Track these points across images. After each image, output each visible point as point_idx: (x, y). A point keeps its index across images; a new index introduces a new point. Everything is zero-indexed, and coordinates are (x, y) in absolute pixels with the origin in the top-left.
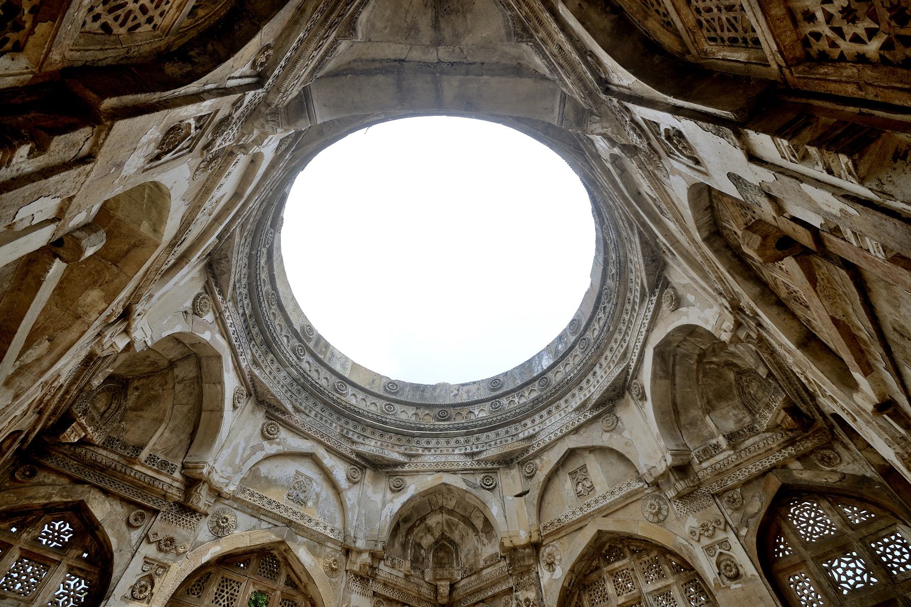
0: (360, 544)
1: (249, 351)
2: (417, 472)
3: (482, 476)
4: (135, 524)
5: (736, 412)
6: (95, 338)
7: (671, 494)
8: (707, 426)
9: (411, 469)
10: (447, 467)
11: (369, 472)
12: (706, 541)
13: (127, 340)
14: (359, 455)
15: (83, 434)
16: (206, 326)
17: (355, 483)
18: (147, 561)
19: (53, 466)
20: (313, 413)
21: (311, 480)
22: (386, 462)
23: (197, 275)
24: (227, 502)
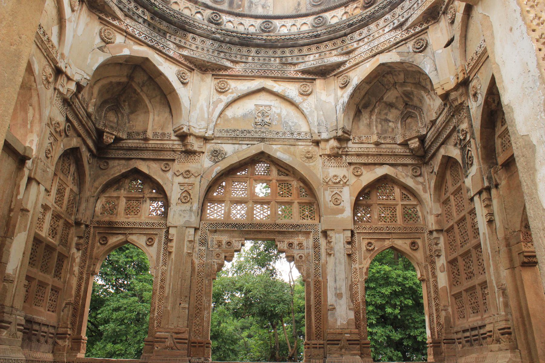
0: (324, 136)
1: (169, 43)
2: (357, 64)
3: (412, 42)
4: (166, 169)
6: (55, 92)
9: (352, 64)
10: (381, 48)
11: (319, 82)
13: (74, 83)
14: (303, 72)
15: (114, 137)
16: (121, 47)
17: (309, 95)
18: (181, 184)
19: (113, 156)
20: (250, 58)
21: (270, 106)
22: (330, 68)
23: (88, 19)
24: (213, 141)
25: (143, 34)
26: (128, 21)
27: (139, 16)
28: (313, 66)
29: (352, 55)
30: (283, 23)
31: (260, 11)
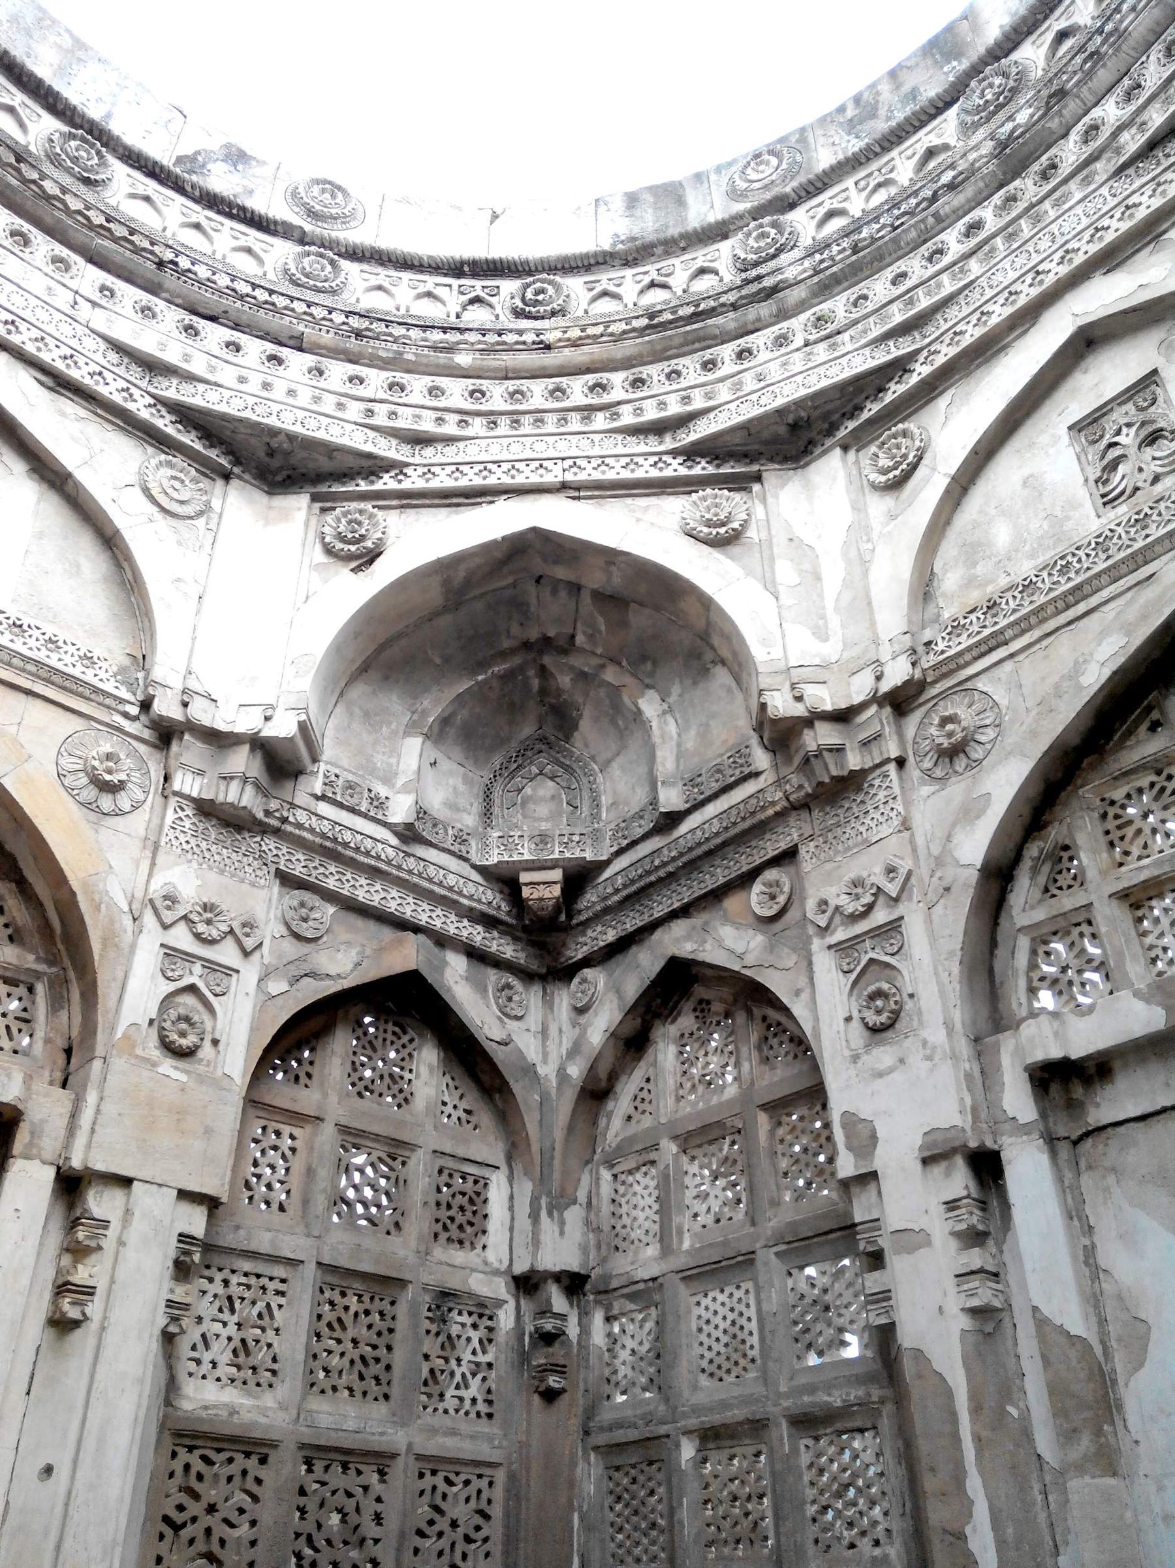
5: (462, 788)
7: (187, 783)
8: (395, 752)
12: (181, 938)
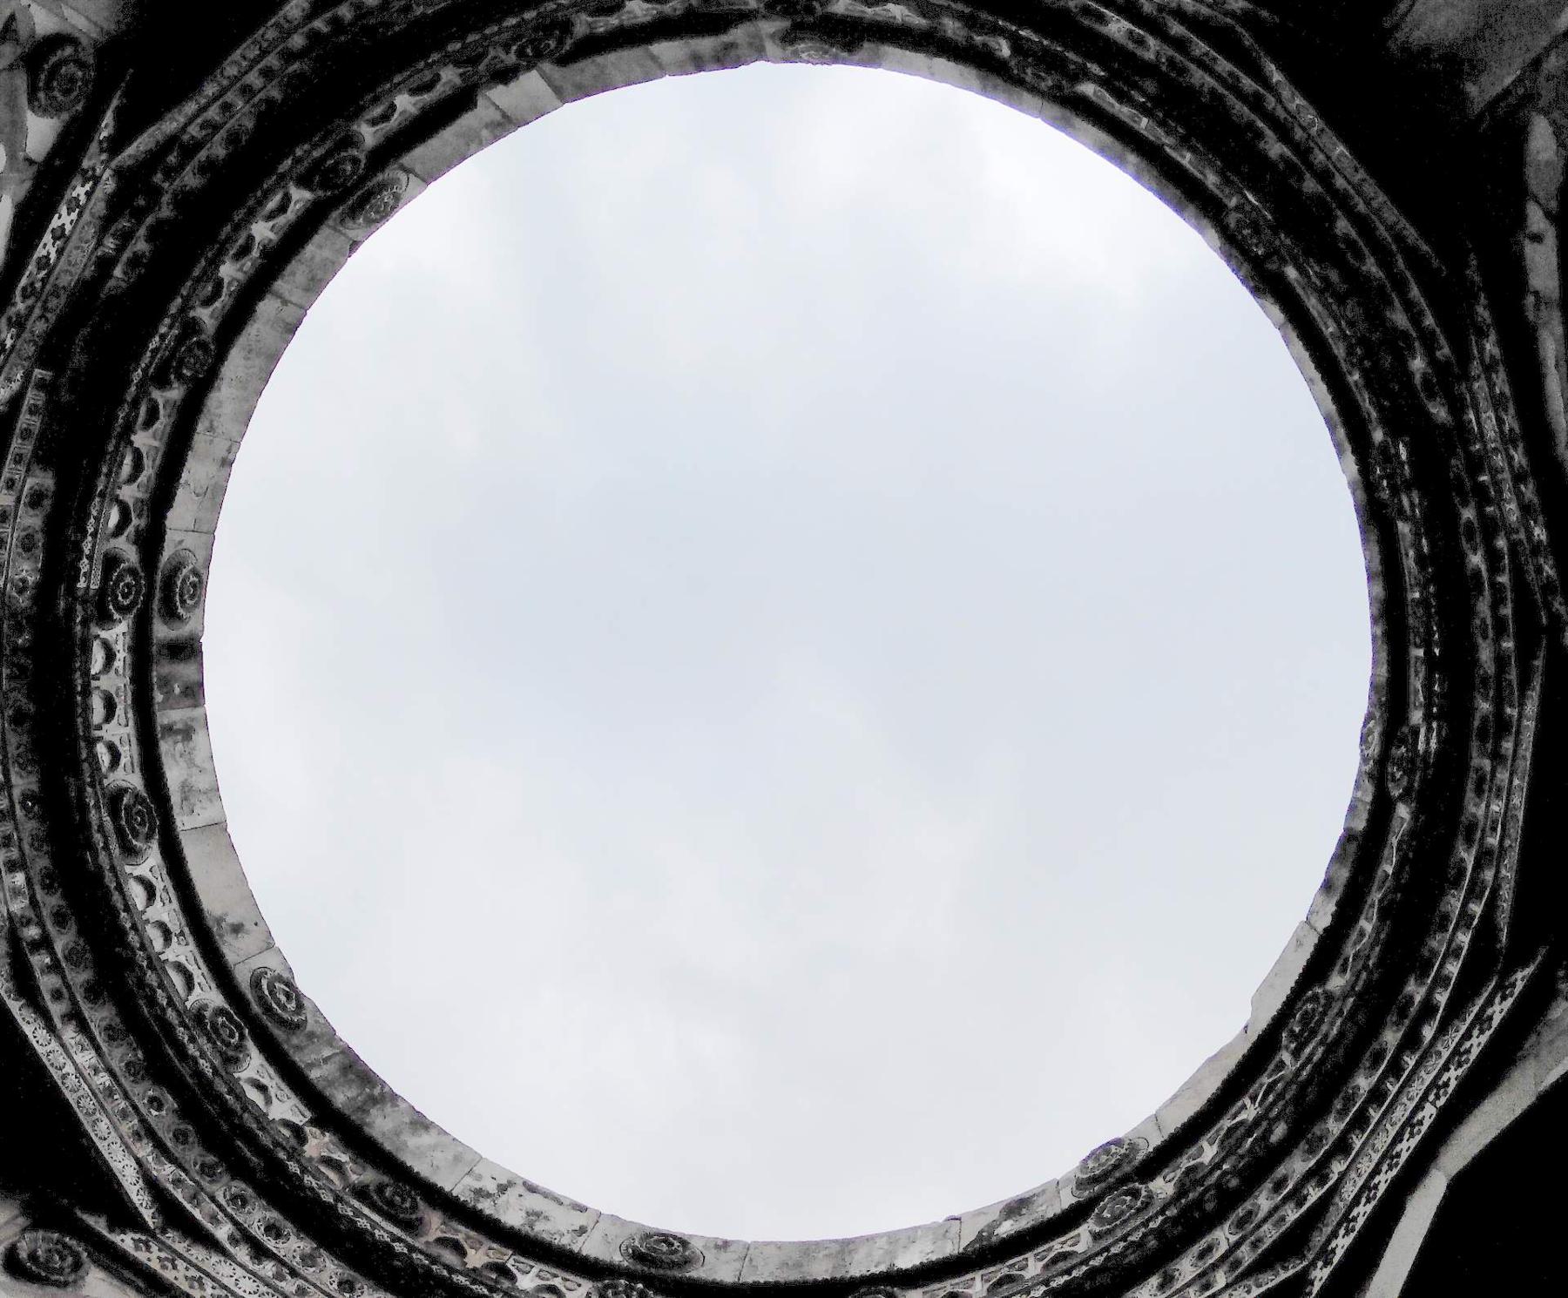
9: (142, 1256)
25: (60, 252)
26: (108, 185)
27: (126, 238)
28: (56, 1075)
29: (173, 1238)
30: (159, 885)
31: (174, 775)
